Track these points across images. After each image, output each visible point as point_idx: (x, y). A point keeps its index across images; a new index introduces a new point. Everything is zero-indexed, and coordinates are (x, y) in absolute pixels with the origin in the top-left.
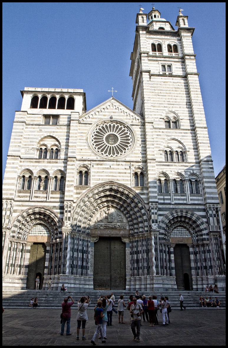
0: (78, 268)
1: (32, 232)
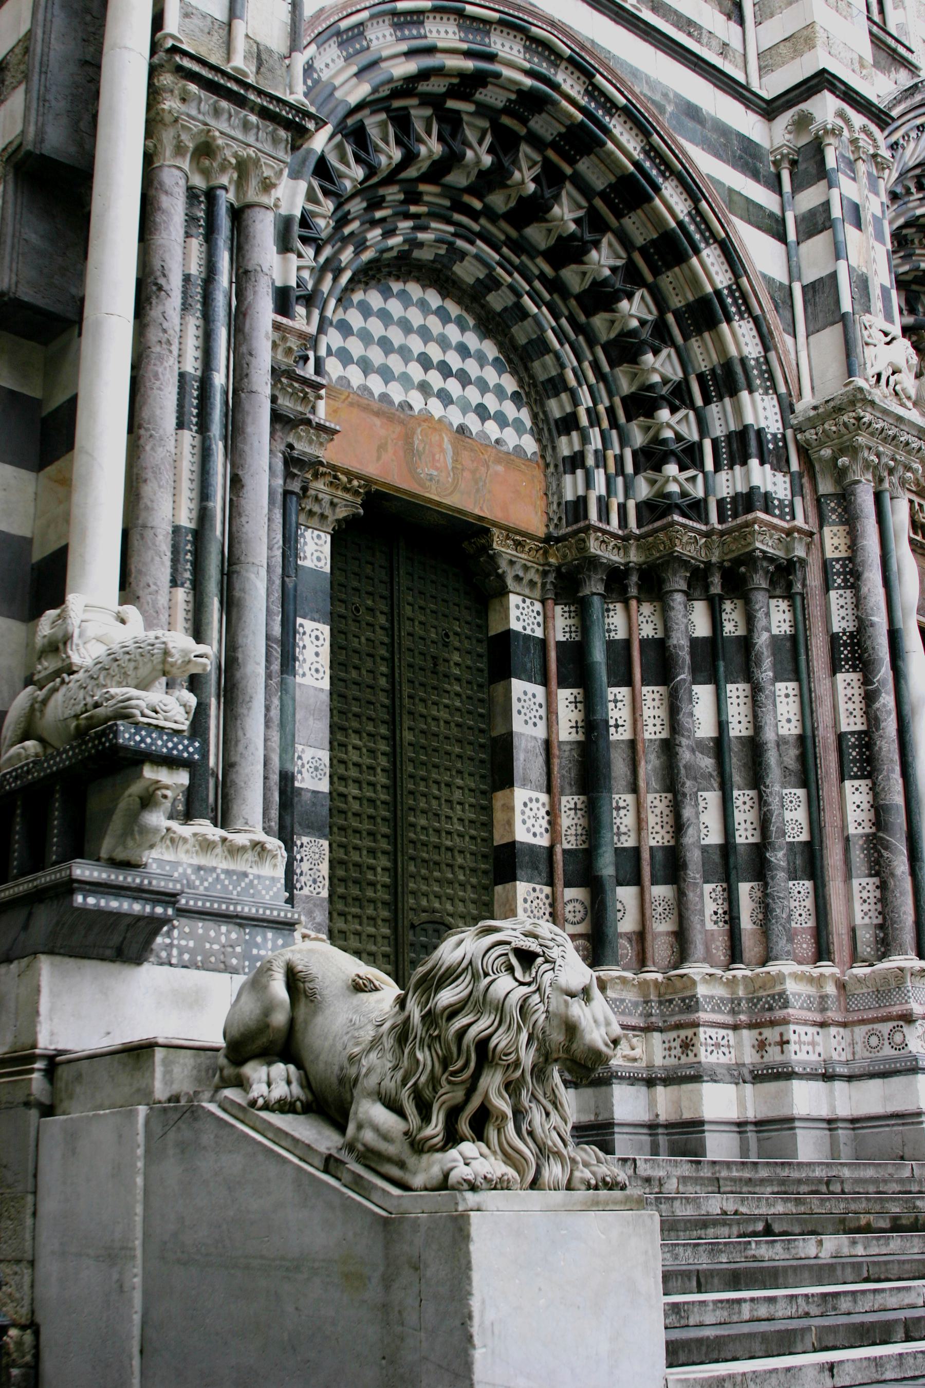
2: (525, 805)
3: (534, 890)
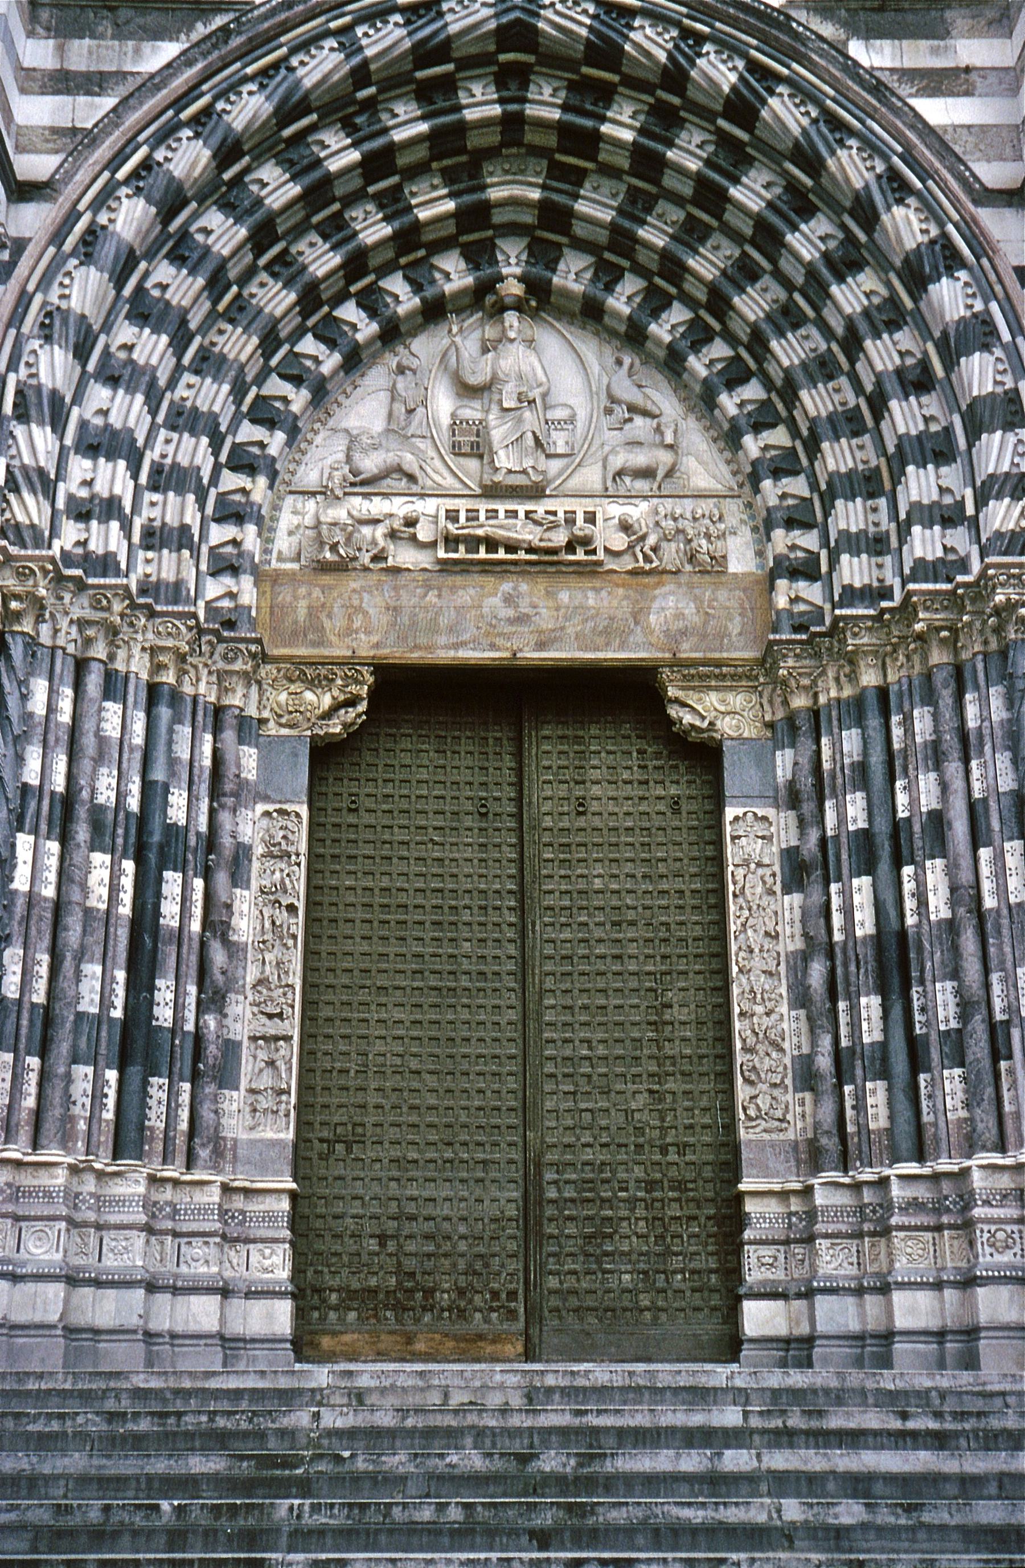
0: (63, 1048)
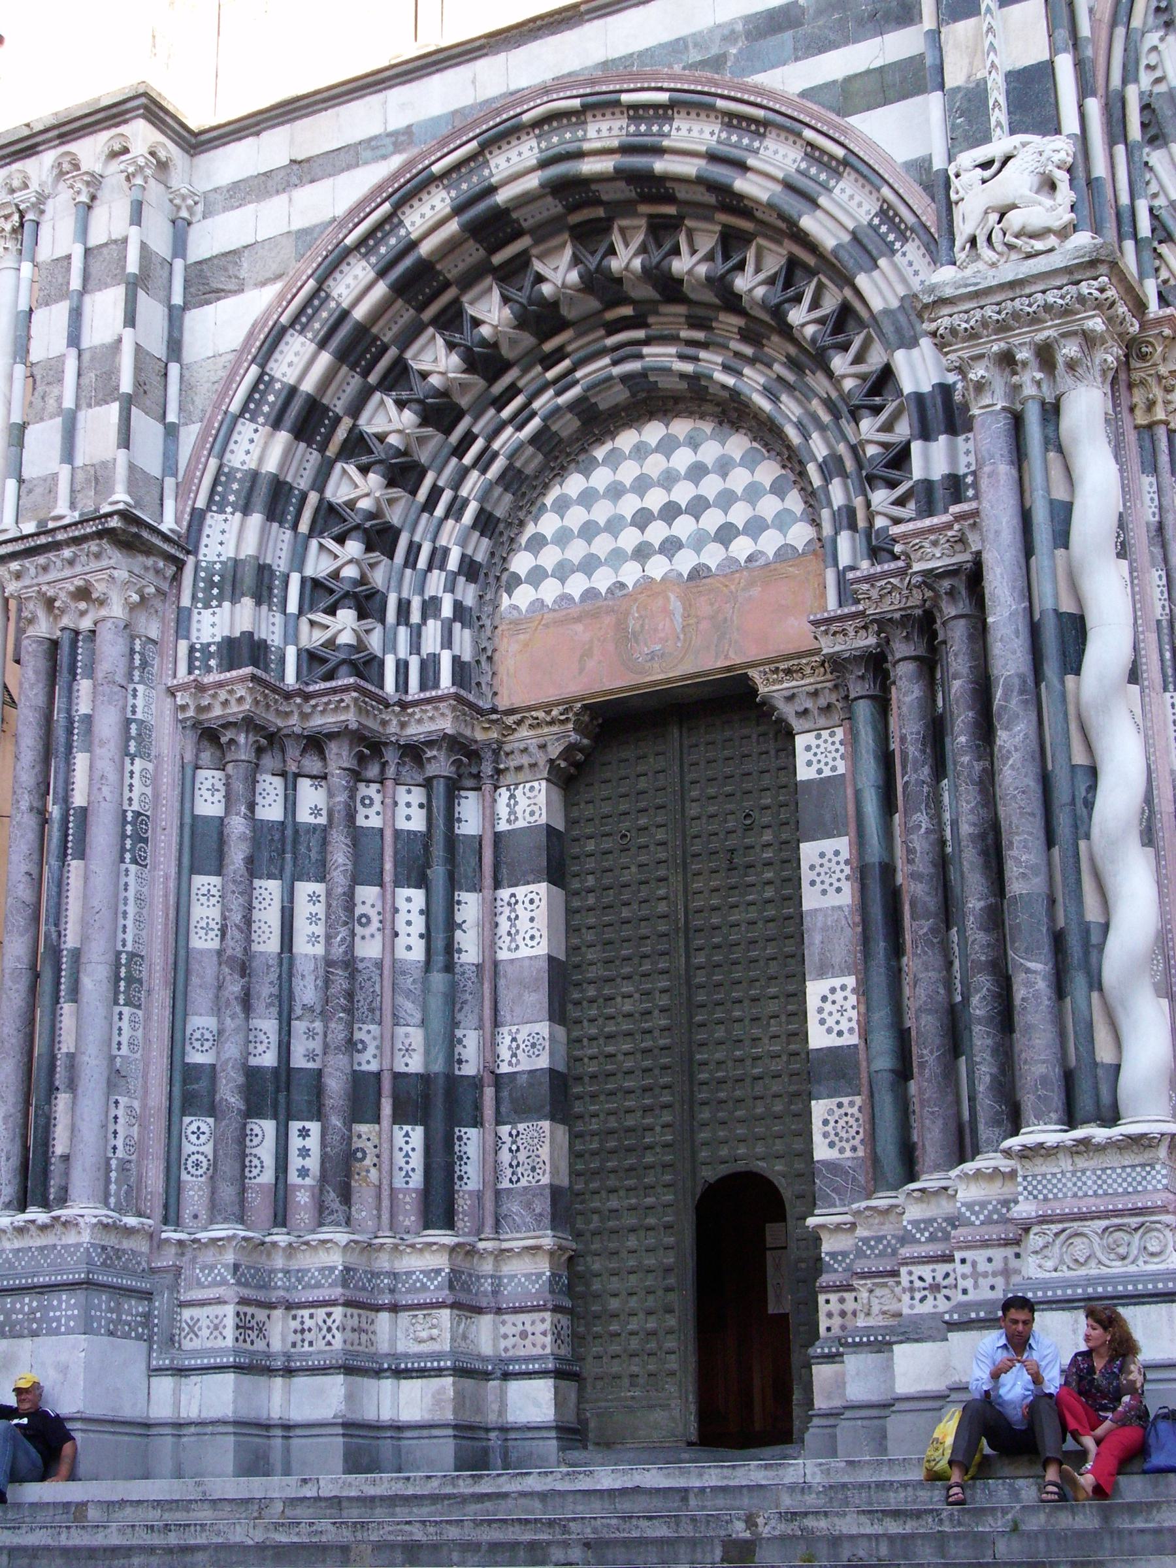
1: (549, 557)
2: (824, 999)
3: (840, 1105)
